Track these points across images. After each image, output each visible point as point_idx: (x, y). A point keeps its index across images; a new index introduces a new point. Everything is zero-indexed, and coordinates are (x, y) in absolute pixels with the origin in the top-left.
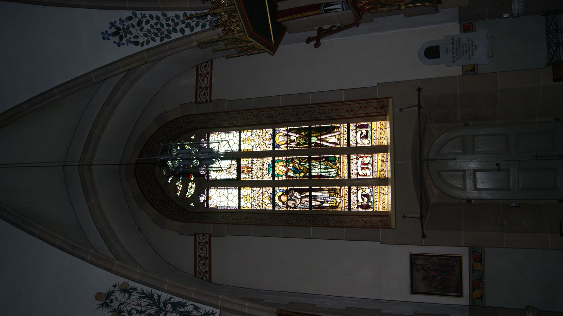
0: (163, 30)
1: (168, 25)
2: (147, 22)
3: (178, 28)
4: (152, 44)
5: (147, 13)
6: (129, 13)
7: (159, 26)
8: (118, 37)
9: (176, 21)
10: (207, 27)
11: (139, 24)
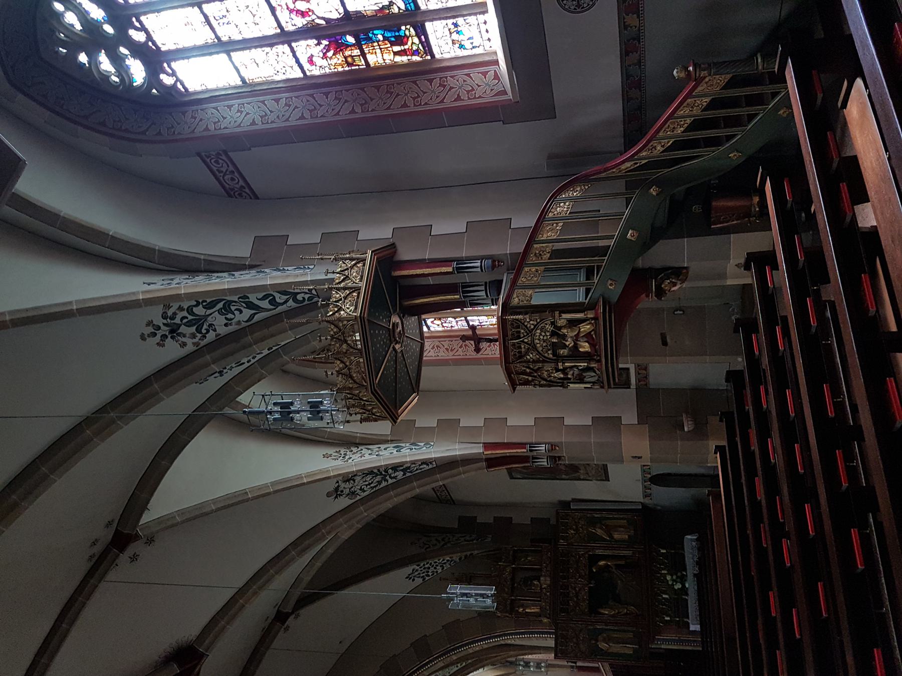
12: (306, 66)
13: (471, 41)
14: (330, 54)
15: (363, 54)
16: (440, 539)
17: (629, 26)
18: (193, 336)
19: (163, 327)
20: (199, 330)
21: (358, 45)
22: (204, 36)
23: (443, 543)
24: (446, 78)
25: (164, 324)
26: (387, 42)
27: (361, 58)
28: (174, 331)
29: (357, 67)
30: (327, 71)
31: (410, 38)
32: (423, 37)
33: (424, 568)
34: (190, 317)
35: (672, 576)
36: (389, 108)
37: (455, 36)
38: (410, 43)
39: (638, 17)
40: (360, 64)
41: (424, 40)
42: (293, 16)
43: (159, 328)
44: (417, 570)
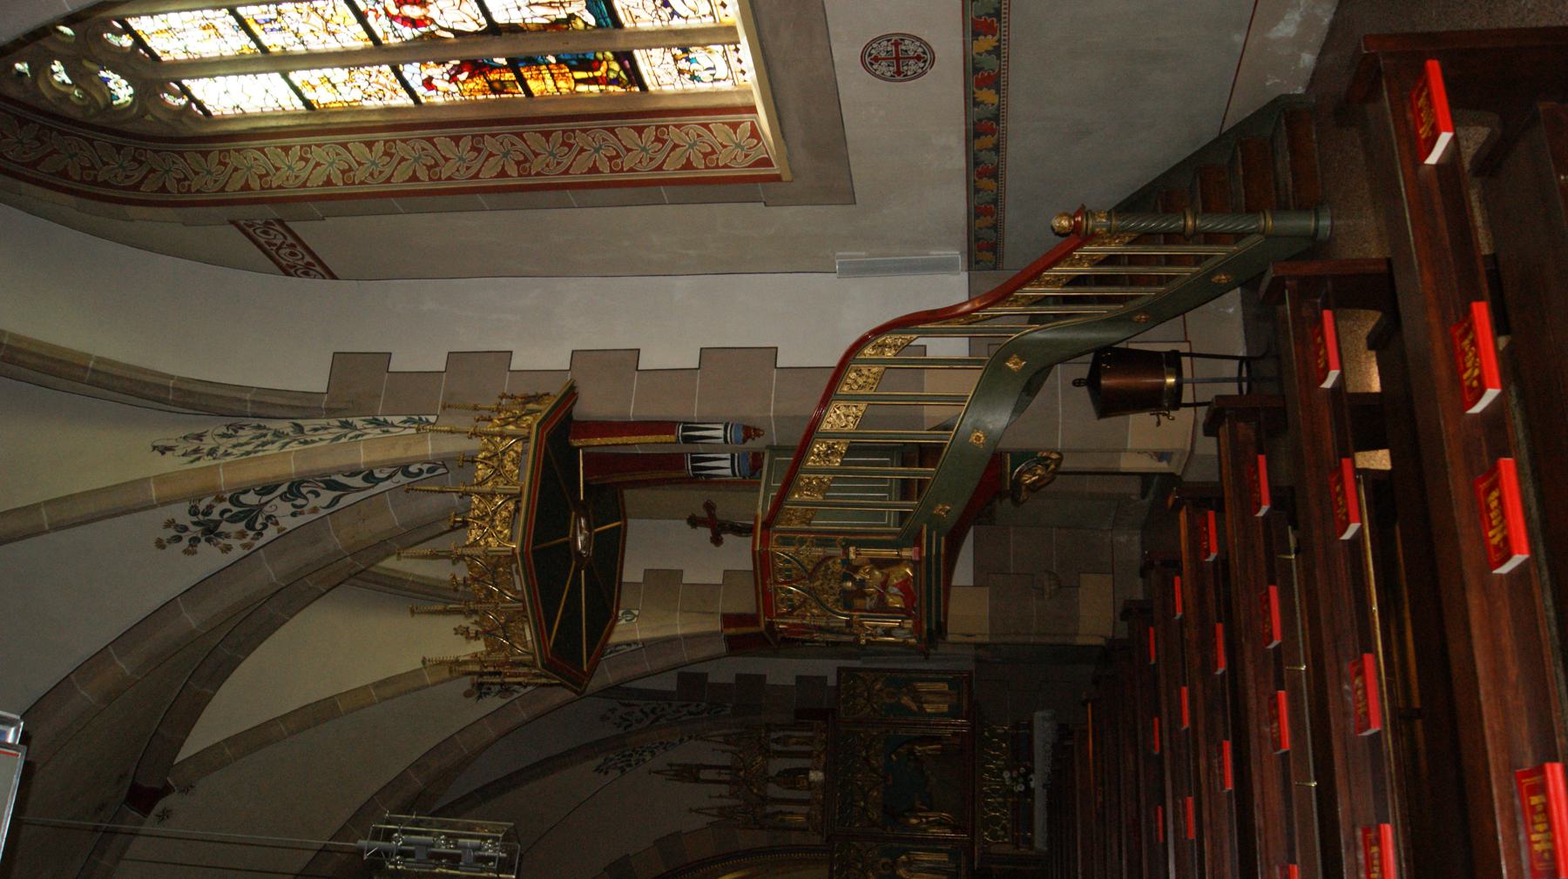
12: (421, 91)
13: (713, 72)
14: (463, 76)
15: (522, 80)
16: (647, 709)
17: (982, 102)
18: (242, 535)
19: (193, 528)
20: (250, 526)
21: (513, 65)
22: (237, 43)
23: (652, 717)
24: (667, 127)
25: (195, 523)
26: (563, 66)
27: (518, 84)
29: (511, 96)
30: (457, 97)
31: (605, 63)
32: (627, 63)
33: (624, 756)
34: (235, 510)
35: (1011, 772)
36: (566, 172)
37: (683, 65)
38: (602, 69)
39: (998, 92)
40: (516, 91)
41: (628, 66)
42: (397, 25)
43: (185, 529)
44: (612, 760)
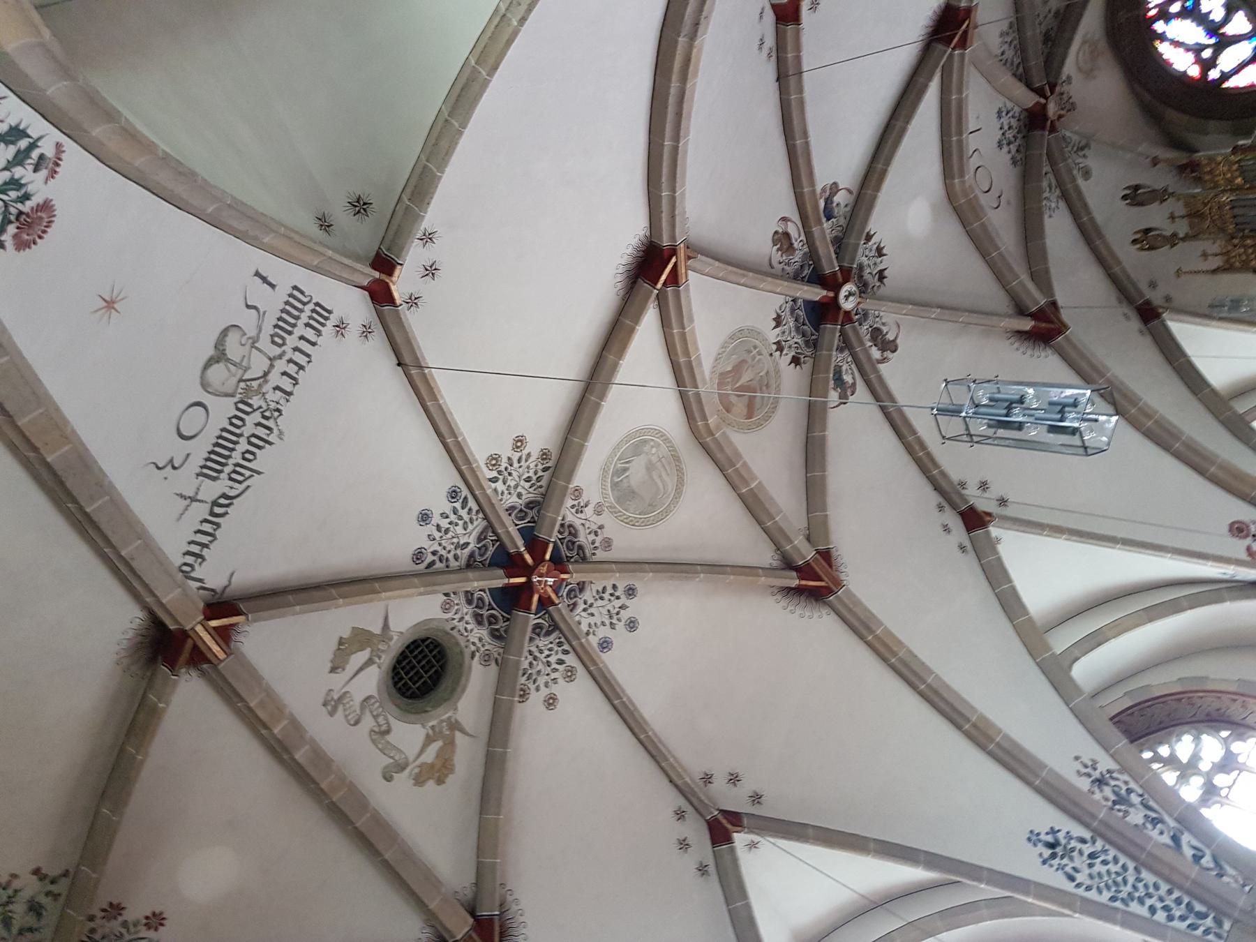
0: (1122, 888)
1: (1134, 887)
2: (1105, 863)
3: (1149, 902)
4: (1093, 895)
5: (1112, 852)
6: (1087, 835)
7: (1120, 879)
8: (1050, 851)
9: (1151, 890)
10: (1199, 932)
11: (1092, 856)
18: (1106, 799)
28: (1100, 782)
43: (1095, 769)
